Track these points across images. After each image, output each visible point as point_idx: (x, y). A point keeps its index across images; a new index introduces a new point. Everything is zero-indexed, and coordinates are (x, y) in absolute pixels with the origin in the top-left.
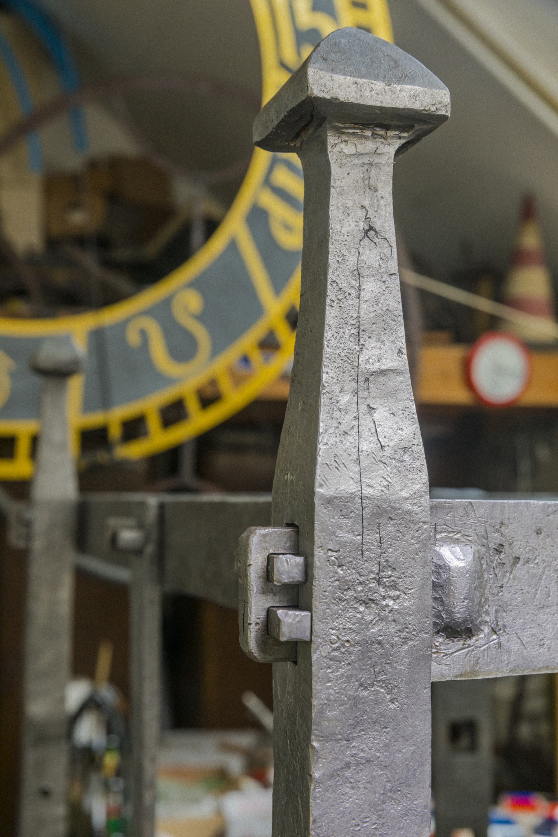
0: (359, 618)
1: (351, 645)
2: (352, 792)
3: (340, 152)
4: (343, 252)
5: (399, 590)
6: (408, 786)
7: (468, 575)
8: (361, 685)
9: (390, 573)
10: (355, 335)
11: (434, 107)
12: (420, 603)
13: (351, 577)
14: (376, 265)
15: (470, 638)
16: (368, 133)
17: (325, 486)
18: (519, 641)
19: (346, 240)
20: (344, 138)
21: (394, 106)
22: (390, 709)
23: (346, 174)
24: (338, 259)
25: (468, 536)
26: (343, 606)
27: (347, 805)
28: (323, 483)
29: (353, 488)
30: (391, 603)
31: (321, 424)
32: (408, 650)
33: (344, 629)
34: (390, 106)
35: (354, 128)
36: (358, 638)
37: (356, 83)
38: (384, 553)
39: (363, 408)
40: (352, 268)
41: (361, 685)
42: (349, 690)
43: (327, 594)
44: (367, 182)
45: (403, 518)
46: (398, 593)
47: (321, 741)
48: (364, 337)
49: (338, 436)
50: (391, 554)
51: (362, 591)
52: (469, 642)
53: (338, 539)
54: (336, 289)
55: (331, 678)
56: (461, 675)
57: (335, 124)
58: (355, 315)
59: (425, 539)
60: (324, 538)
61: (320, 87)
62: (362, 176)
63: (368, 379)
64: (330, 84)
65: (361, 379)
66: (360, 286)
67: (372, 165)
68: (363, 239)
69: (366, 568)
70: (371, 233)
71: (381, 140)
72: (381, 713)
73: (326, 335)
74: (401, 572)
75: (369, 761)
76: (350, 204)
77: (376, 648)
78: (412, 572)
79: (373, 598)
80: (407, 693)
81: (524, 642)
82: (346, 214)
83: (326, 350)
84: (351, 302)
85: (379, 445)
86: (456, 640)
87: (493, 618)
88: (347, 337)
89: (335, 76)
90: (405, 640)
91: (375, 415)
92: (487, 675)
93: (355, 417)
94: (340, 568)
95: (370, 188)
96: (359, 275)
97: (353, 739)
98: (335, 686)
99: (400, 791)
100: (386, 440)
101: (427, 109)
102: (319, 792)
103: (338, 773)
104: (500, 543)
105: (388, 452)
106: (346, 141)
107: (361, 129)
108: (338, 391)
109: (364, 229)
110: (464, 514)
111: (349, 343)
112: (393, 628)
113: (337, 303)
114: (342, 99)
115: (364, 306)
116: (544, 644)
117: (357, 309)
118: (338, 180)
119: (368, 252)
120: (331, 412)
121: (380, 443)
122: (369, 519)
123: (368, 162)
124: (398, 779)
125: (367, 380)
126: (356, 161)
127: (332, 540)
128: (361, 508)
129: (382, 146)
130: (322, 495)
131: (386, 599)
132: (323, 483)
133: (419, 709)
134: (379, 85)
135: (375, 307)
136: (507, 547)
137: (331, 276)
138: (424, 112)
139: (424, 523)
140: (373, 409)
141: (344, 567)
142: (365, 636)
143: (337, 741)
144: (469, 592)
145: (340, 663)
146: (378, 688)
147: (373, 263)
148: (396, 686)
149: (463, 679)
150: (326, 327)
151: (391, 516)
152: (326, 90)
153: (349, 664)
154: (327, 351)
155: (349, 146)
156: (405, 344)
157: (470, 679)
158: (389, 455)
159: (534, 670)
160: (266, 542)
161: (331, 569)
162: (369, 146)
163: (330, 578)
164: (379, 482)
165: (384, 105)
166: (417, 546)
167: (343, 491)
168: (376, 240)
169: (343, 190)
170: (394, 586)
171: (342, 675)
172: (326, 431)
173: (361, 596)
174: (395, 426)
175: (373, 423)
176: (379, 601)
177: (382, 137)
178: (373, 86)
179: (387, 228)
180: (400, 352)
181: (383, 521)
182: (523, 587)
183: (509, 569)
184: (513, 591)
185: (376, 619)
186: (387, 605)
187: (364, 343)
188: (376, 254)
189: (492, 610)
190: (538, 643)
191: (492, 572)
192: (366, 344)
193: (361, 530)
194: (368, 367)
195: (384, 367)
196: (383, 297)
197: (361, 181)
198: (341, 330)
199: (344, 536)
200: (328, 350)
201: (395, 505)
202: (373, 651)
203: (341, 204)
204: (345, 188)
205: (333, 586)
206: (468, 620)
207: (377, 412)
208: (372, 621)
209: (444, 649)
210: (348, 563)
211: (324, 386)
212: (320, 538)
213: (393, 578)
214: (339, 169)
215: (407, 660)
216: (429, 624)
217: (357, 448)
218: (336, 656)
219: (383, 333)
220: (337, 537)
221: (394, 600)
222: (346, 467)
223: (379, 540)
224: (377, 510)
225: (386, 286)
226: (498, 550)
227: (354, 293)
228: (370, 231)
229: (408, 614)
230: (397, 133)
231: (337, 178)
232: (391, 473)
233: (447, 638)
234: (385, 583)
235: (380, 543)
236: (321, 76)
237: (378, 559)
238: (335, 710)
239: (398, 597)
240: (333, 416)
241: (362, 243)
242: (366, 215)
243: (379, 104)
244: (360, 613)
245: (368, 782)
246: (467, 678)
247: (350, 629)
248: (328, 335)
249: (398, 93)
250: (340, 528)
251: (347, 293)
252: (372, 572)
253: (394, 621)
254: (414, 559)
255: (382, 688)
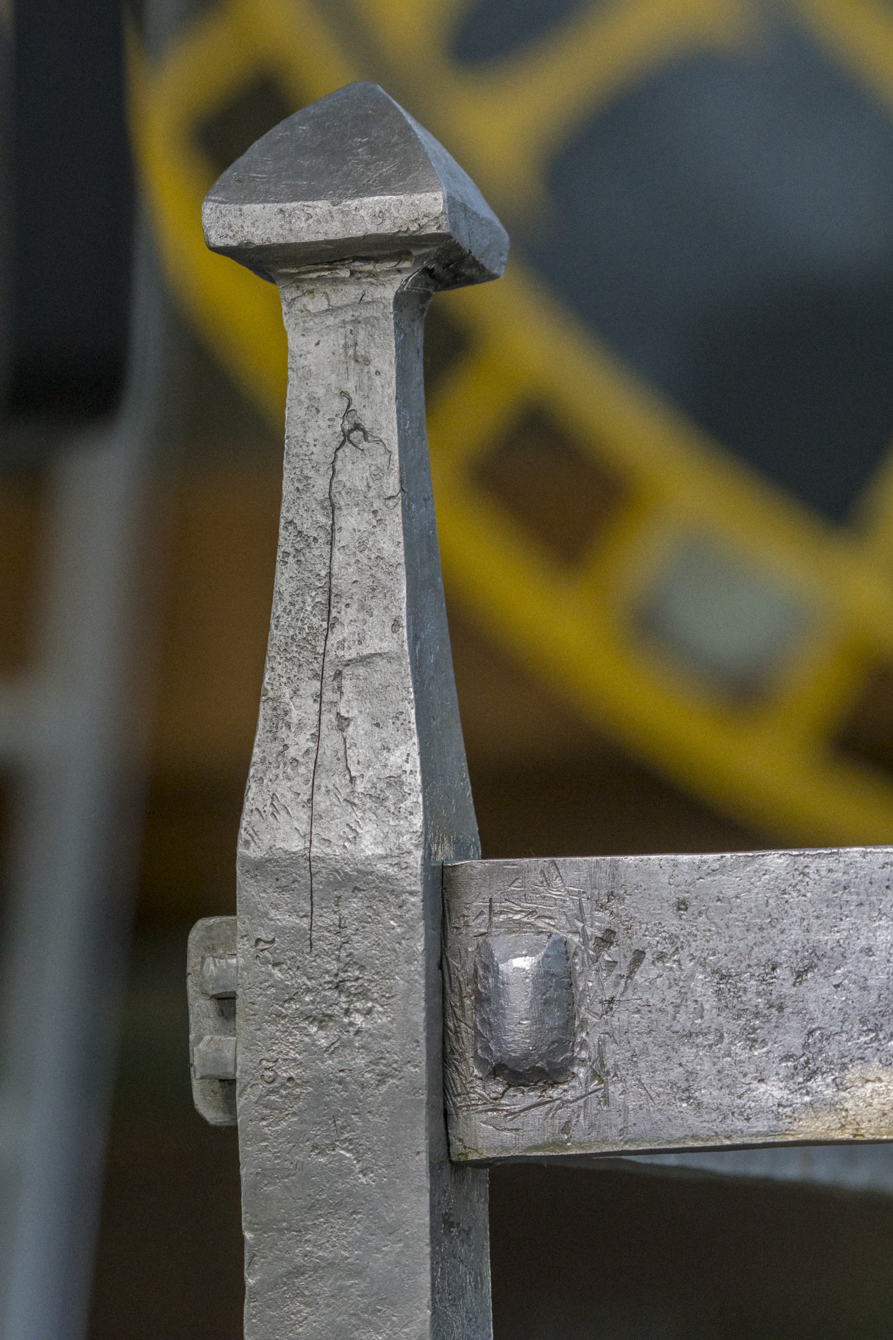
0: (308, 1043)
1: (297, 1085)
2: (309, 1310)
3: (302, 311)
4: (305, 472)
5: (372, 1000)
6: (393, 1304)
7: (528, 980)
8: (315, 1147)
9: (357, 973)
10: (323, 604)
11: (416, 225)
12: (404, 1019)
13: (294, 981)
14: (361, 486)
15: (552, 1086)
16: (345, 273)
17: (252, 844)
18: (644, 1092)
19: (312, 453)
20: (307, 287)
21: (346, 237)
22: (362, 1183)
23: (313, 345)
24: (297, 484)
25: (550, 918)
26: (283, 1025)
27: (301, 1330)
28: (249, 838)
29: (296, 845)
30: (358, 1019)
31: (256, 750)
32: (386, 1093)
33: (285, 1060)
34: (340, 236)
35: (318, 271)
36: (307, 1074)
37: (281, 211)
38: (347, 942)
39: (328, 718)
40: (320, 496)
41: (315, 1147)
42: (296, 1154)
43: (256, 1007)
44: (351, 352)
45: (377, 887)
46: (370, 1004)
47: (256, 1230)
48: (339, 606)
49: (281, 766)
50: (359, 946)
51: (313, 1002)
52: (554, 1093)
53: (272, 922)
54: (293, 534)
55: (266, 1134)
56: (536, 1148)
57: (281, 271)
58: (323, 573)
59: (412, 919)
60: (252, 924)
61: (221, 230)
62: (343, 342)
63: (341, 672)
64: (237, 222)
65: (329, 672)
66: (333, 524)
67: (359, 322)
68: (341, 446)
69: (319, 967)
70: (356, 435)
71: (369, 279)
72: (348, 1190)
73: (274, 610)
74: (373, 971)
75: (332, 1265)
76: (321, 392)
77: (336, 1090)
78: (392, 971)
79: (329, 1012)
80: (387, 1159)
81: (653, 1094)
82: (313, 409)
83: (274, 632)
84: (317, 553)
85: (348, 777)
86: (526, 1089)
87: (594, 1055)
88: (309, 609)
89: (246, 208)
90: (383, 1078)
91: (351, 729)
92: (583, 1148)
93: (312, 734)
94: (277, 968)
95: (357, 361)
96: (331, 507)
97: (307, 1229)
98: (274, 1147)
99: (380, 1311)
100: (360, 767)
101: (404, 229)
102: (254, 1307)
103: (285, 1280)
104: (607, 926)
105: (360, 787)
106: (311, 292)
107: (329, 269)
108: (288, 696)
109: (343, 431)
110: (542, 882)
111: (312, 618)
112: (361, 1061)
113: (294, 557)
114: (257, 241)
115: (338, 556)
116: (689, 1098)
117: (328, 562)
118: (301, 356)
119: (349, 467)
120: (274, 730)
121: (350, 772)
122: (321, 890)
123: (353, 318)
124: (377, 1294)
125: (339, 674)
126: (330, 321)
127: (262, 925)
128: (309, 875)
129: (372, 289)
130: (247, 859)
131: (352, 1013)
132: (249, 838)
133: (408, 1184)
134: (321, 206)
135: (360, 556)
136: (621, 936)
137: (285, 514)
138: (400, 235)
139: (412, 893)
140: (346, 719)
141: (284, 966)
142: (317, 1071)
143: (281, 1231)
144: (531, 1007)
145: (281, 1113)
146: (342, 1152)
147: (358, 483)
148: (369, 1149)
149: (539, 1154)
150: (276, 597)
151: (358, 885)
152: (231, 234)
153: (294, 1114)
154: (277, 636)
155: (316, 299)
156: (404, 610)
157: (551, 1154)
158: (362, 790)
159: (669, 1142)
160: (210, 938)
161: (263, 969)
162: (352, 292)
163: (261, 983)
164: (341, 833)
165: (331, 237)
166: (399, 930)
167: (280, 851)
168: (365, 445)
169: (310, 371)
170: (364, 994)
171: (284, 1130)
172: (263, 760)
173: (311, 1010)
174: (379, 745)
175: (341, 741)
176: (339, 1016)
177: (371, 274)
178: (310, 211)
179: (384, 424)
180: (396, 624)
181: (345, 893)
182: (652, 1002)
183: (625, 972)
184: (632, 1009)
185: (336, 1045)
186: (351, 1024)
187: (338, 616)
188: (363, 468)
189: (593, 1041)
190: (677, 1097)
191: (593, 977)
192: (342, 617)
193: (309, 909)
194: (341, 653)
195: (366, 652)
196: (373, 538)
197: (341, 351)
198: (300, 599)
199: (286, 920)
200: (275, 631)
201: (360, 867)
202: (332, 1095)
203: (305, 395)
204: (312, 368)
205: (266, 996)
206: (531, 1055)
207: (353, 723)
208: (330, 1047)
209: (507, 1105)
210: (289, 960)
211: (266, 690)
212: (244, 923)
213: (360, 981)
214: (302, 339)
215: (386, 1109)
216: (421, 1051)
217: (311, 782)
218: (274, 1102)
219: (371, 595)
220: (271, 920)
221: (365, 1015)
222: (288, 813)
223: (337, 922)
224: (335, 877)
225: (379, 518)
226: (607, 939)
227: (323, 538)
228: (353, 432)
229: (387, 1038)
230: (393, 264)
231: (299, 353)
232: (362, 818)
233: (510, 1086)
234: (348, 989)
235: (340, 926)
236: (223, 212)
237: (337, 953)
238: (275, 1184)
239: (369, 1011)
240: (278, 734)
241: (340, 454)
242: (349, 406)
243: (321, 237)
244: (310, 1035)
245: (332, 1296)
246: (548, 1153)
247: (294, 1060)
248: (278, 609)
249: (354, 212)
250: (276, 907)
251: (312, 539)
252: (328, 972)
253: (363, 1047)
254: (395, 951)
255: (349, 1151)
